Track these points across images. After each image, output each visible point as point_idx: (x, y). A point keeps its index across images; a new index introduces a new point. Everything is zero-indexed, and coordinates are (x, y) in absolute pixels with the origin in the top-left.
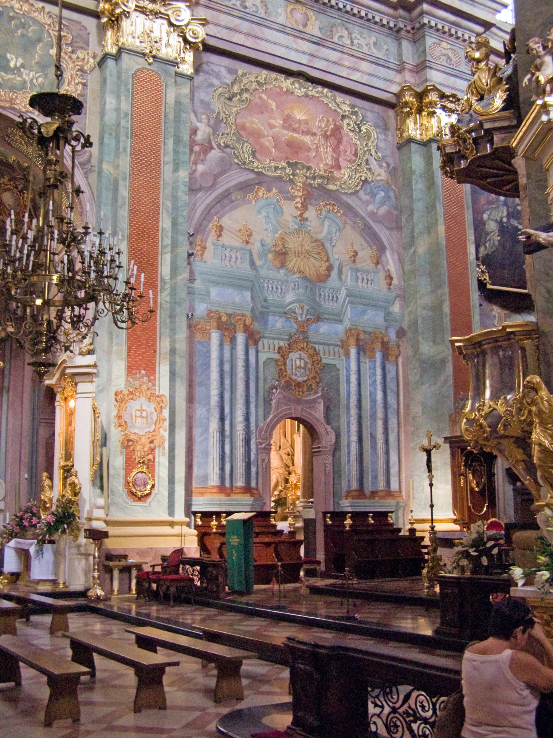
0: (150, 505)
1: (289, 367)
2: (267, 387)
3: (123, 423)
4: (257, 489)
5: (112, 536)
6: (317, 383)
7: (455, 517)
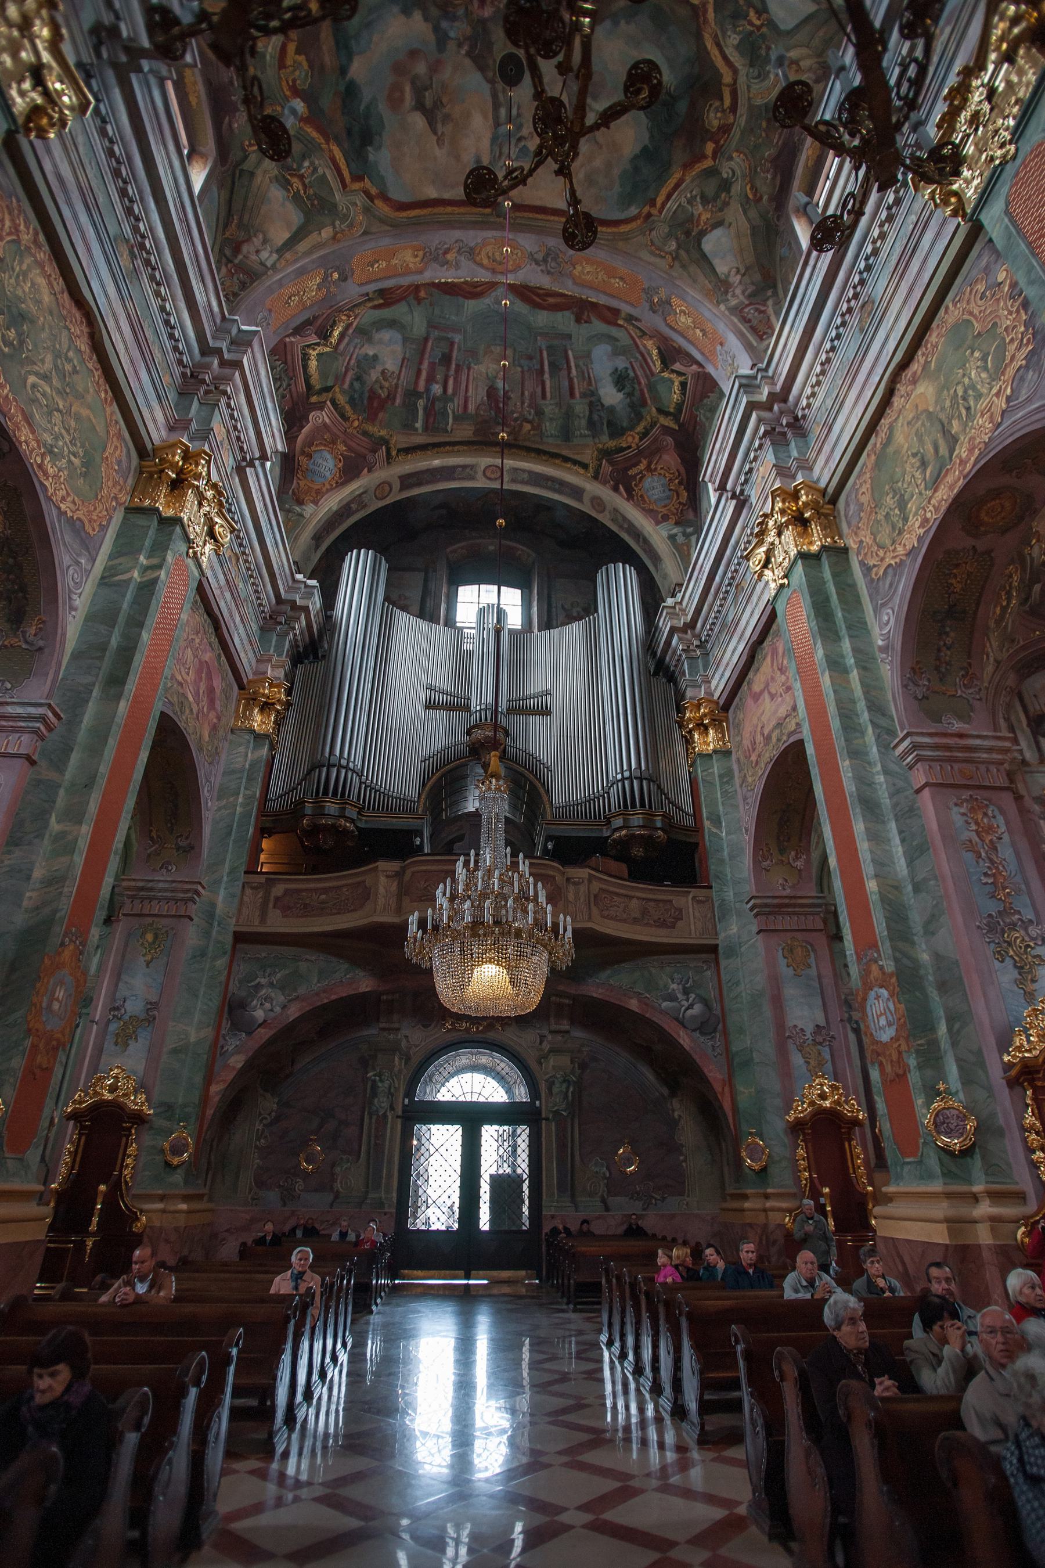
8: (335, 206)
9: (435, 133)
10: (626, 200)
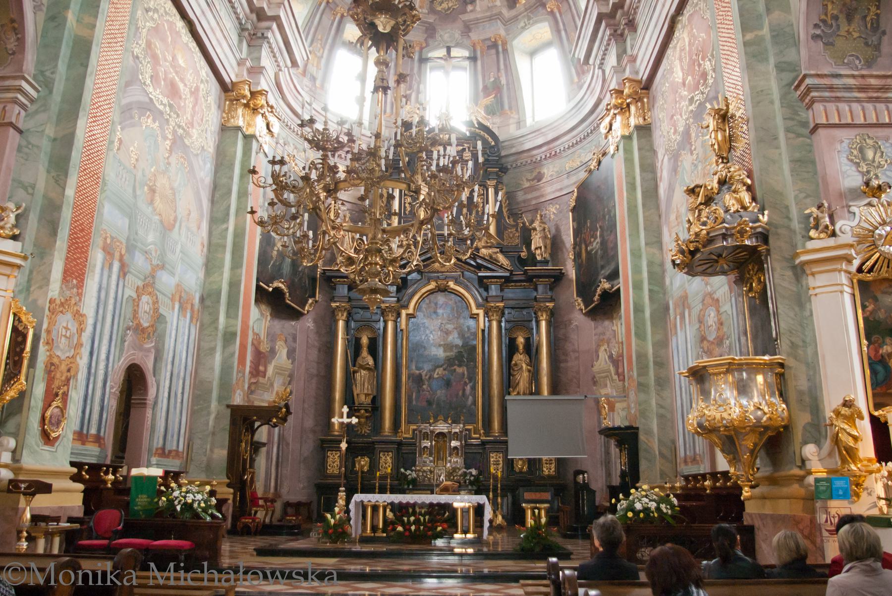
0: (56, 451)
1: (140, 310)
2: (125, 326)
3: (50, 341)
4: (104, 439)
5: (58, 491)
6: (154, 332)
7: (228, 481)
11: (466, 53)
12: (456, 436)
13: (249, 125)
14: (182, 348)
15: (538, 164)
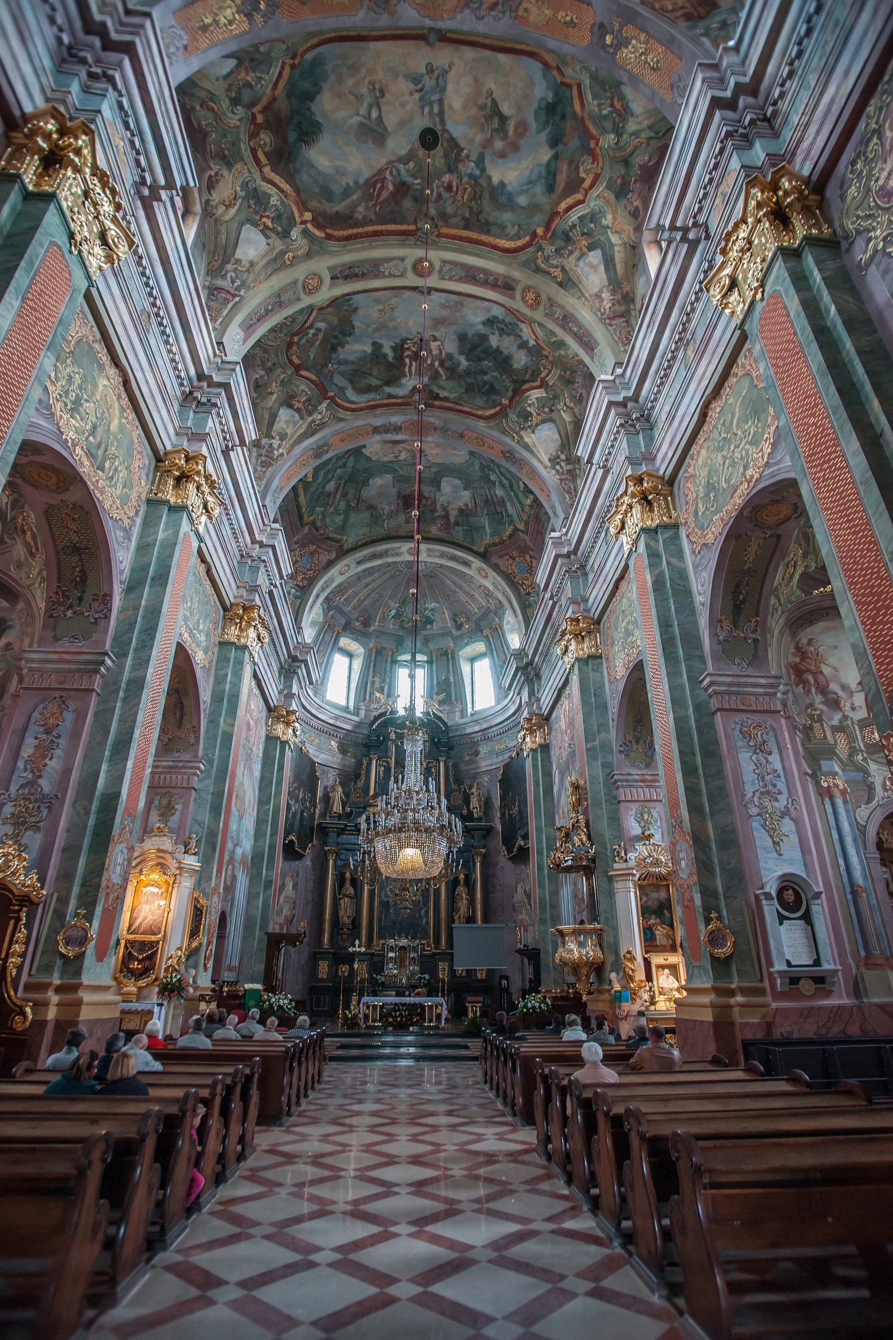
8: (591, 77)
9: (494, 100)
10: (317, 63)
11: (425, 658)
12: (414, 949)
13: (284, 733)
14: (242, 894)
15: (476, 744)
